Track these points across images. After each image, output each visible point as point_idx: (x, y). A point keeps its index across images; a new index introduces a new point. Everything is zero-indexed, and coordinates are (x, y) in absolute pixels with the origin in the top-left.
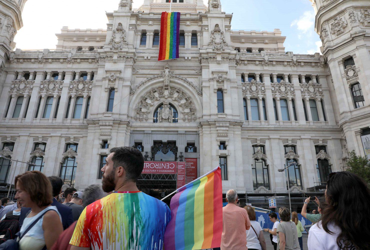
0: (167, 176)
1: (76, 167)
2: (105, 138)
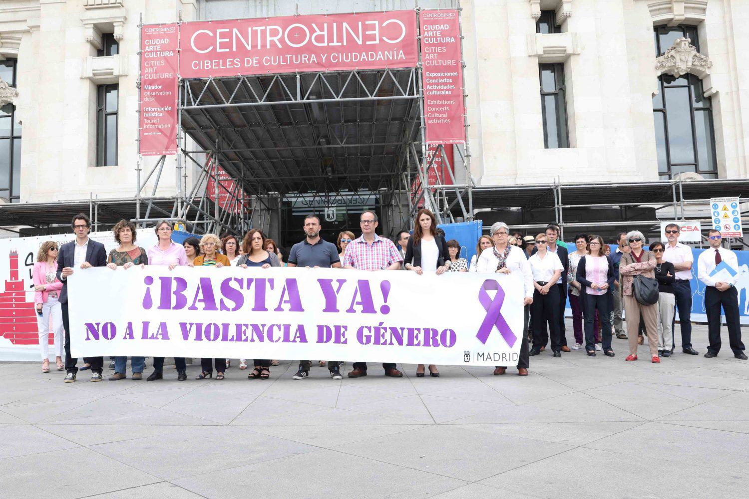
0: (371, 78)
1: (20, 137)
2: (102, 16)
